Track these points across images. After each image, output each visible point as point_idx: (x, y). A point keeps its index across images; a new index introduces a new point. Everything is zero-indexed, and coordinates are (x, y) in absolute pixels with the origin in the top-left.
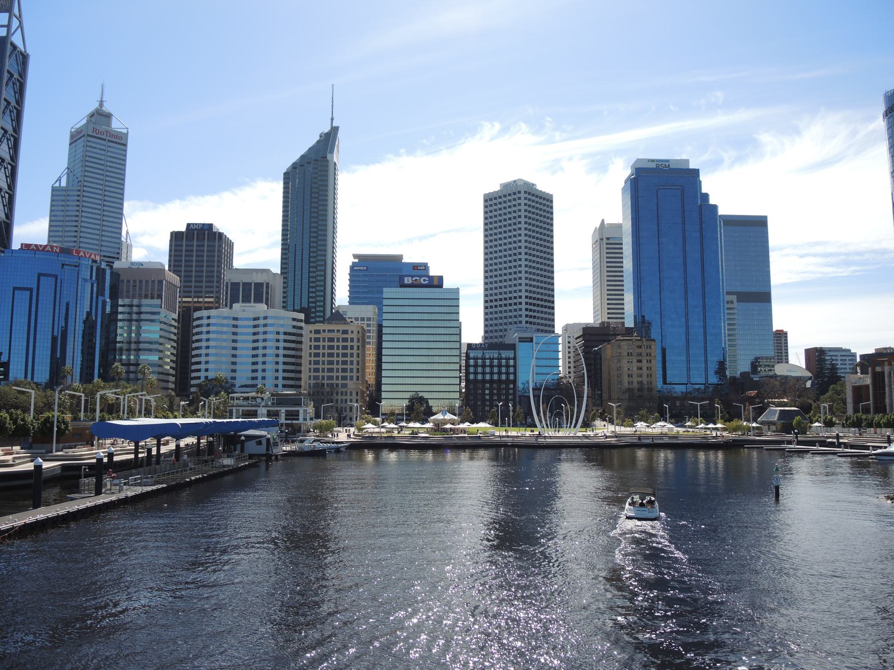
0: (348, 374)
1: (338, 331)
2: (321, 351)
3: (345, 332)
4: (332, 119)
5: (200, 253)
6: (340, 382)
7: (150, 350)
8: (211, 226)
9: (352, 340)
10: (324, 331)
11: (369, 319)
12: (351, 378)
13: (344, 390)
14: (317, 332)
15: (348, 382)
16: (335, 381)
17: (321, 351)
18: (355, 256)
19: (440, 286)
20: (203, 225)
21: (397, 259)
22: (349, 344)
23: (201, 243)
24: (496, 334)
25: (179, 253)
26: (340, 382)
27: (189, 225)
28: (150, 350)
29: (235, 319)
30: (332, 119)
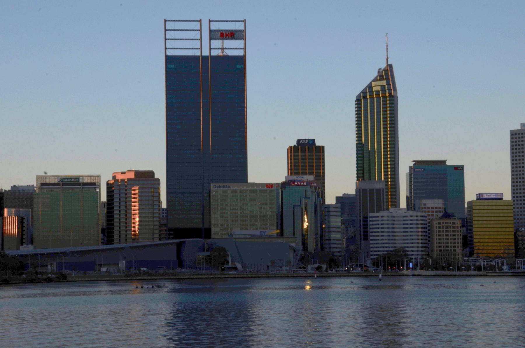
0: (456, 245)
1: (450, 223)
2: (442, 233)
3: (454, 223)
4: (387, 59)
5: (303, 157)
6: (452, 249)
7: (335, 232)
8: (313, 141)
9: (458, 227)
10: (443, 223)
11: (440, 208)
12: (458, 247)
13: (455, 253)
14: (439, 223)
15: (457, 249)
16: (449, 249)
17: (442, 233)
18: (414, 161)
19: (501, 199)
20: (309, 140)
21: (444, 162)
22: (456, 229)
23: (311, 154)
24: (521, 217)
25: (297, 161)
26: (452, 249)
27: (299, 141)
28: (335, 232)
29: (394, 217)
30: (387, 59)
